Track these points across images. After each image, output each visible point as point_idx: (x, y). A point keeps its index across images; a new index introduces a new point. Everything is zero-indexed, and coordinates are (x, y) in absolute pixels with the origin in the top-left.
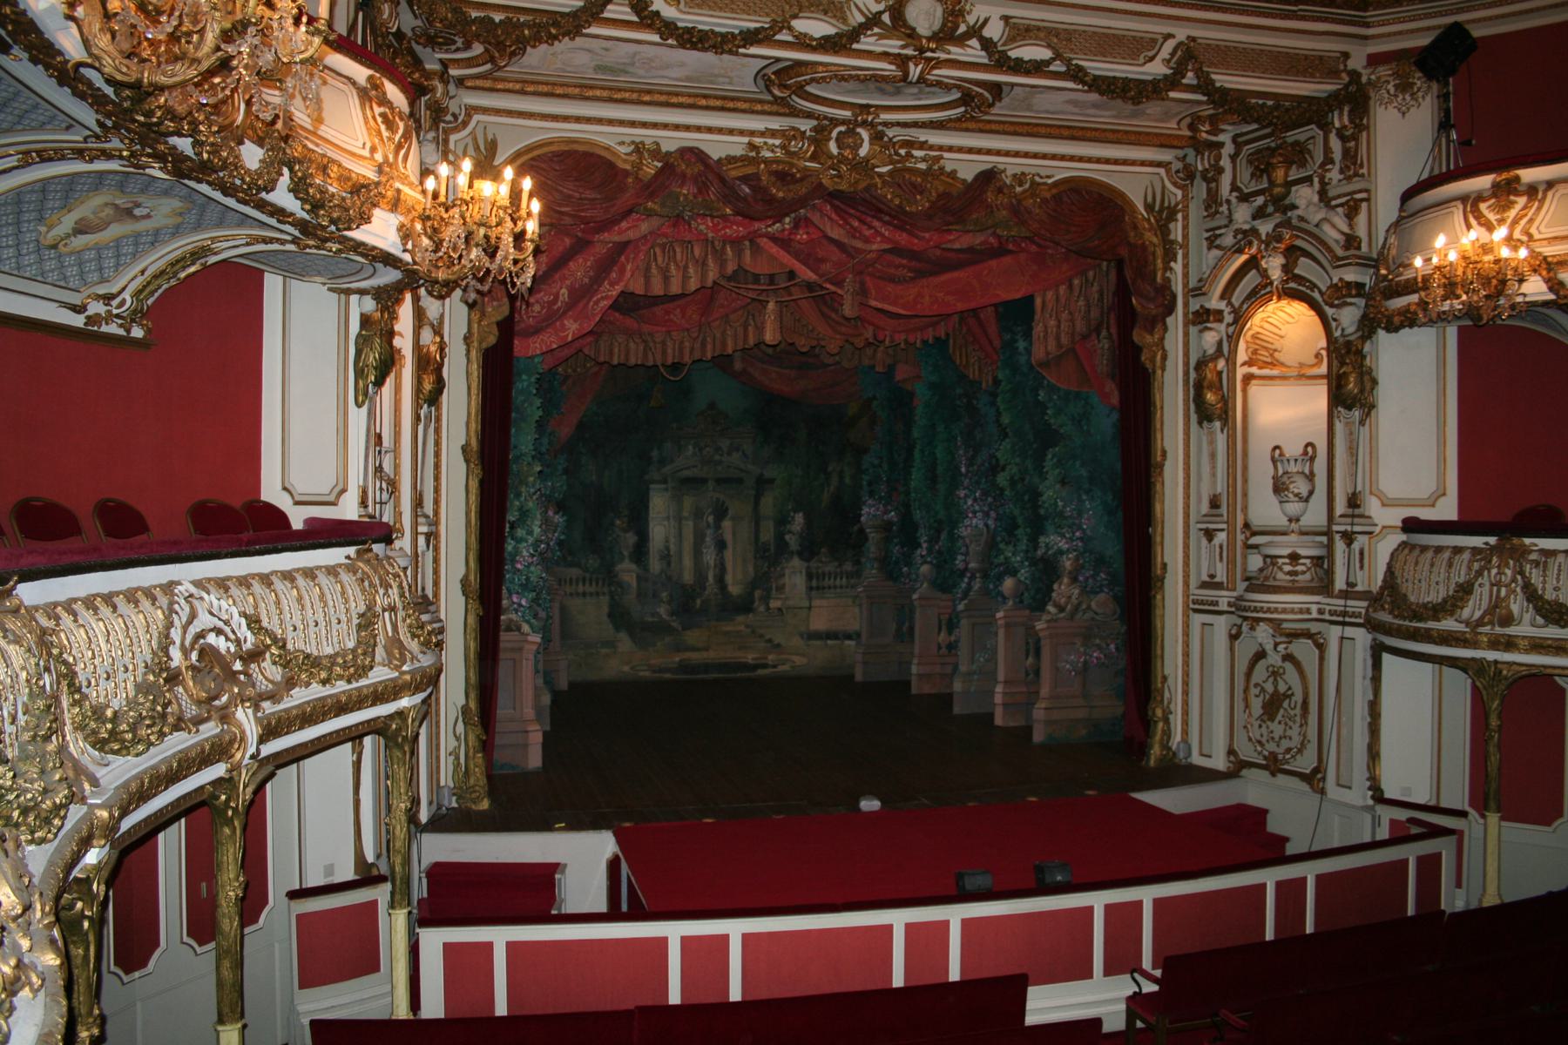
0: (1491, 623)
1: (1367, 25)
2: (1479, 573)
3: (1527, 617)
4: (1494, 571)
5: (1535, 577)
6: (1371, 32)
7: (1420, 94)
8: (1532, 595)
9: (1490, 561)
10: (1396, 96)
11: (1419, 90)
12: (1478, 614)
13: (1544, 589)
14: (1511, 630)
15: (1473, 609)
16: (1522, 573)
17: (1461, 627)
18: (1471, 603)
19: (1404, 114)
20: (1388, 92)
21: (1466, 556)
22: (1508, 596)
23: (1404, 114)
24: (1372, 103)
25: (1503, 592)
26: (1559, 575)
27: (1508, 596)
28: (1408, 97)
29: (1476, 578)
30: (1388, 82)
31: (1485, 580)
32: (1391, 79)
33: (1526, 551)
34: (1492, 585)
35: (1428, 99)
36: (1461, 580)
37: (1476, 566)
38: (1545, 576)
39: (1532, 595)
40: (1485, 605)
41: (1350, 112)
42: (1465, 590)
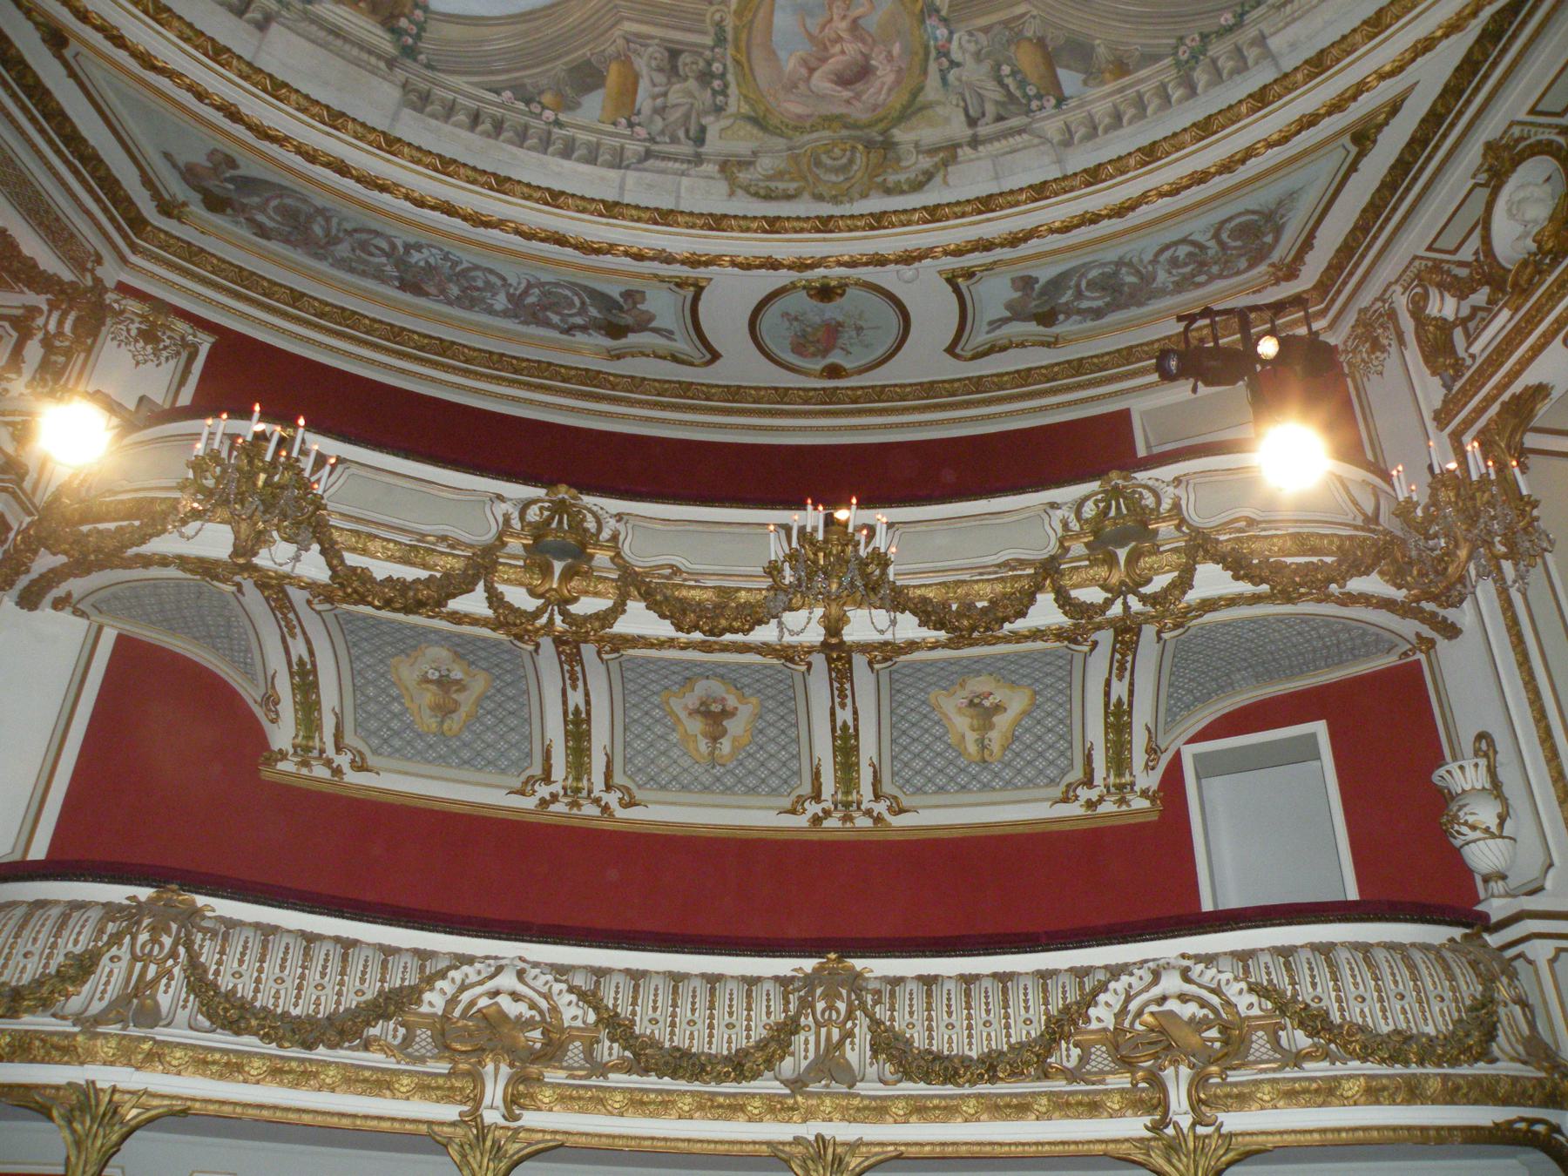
0: (122, 1020)
1: (134, 248)
2: (116, 939)
3: (182, 1015)
4: (144, 937)
5: (208, 955)
6: (134, 259)
7: (165, 354)
8: (199, 983)
9: (139, 923)
10: (136, 341)
11: (165, 348)
12: (97, 1007)
13: (217, 973)
14: (161, 1033)
15: (90, 996)
16: (189, 945)
17: (67, 1027)
18: (86, 988)
19: (138, 363)
20: (128, 331)
21: (94, 915)
22: (157, 980)
23: (138, 363)
24: (104, 330)
25: (152, 970)
26: (243, 954)
27: (157, 980)
28: (149, 348)
29: (109, 944)
30: (133, 322)
31: (124, 952)
32: (137, 319)
33: (196, 913)
34: (135, 958)
35: (172, 363)
36: (78, 950)
37: (111, 928)
38: (222, 952)
39: (199, 983)
40: (112, 991)
41: (78, 319)
42: (84, 966)
